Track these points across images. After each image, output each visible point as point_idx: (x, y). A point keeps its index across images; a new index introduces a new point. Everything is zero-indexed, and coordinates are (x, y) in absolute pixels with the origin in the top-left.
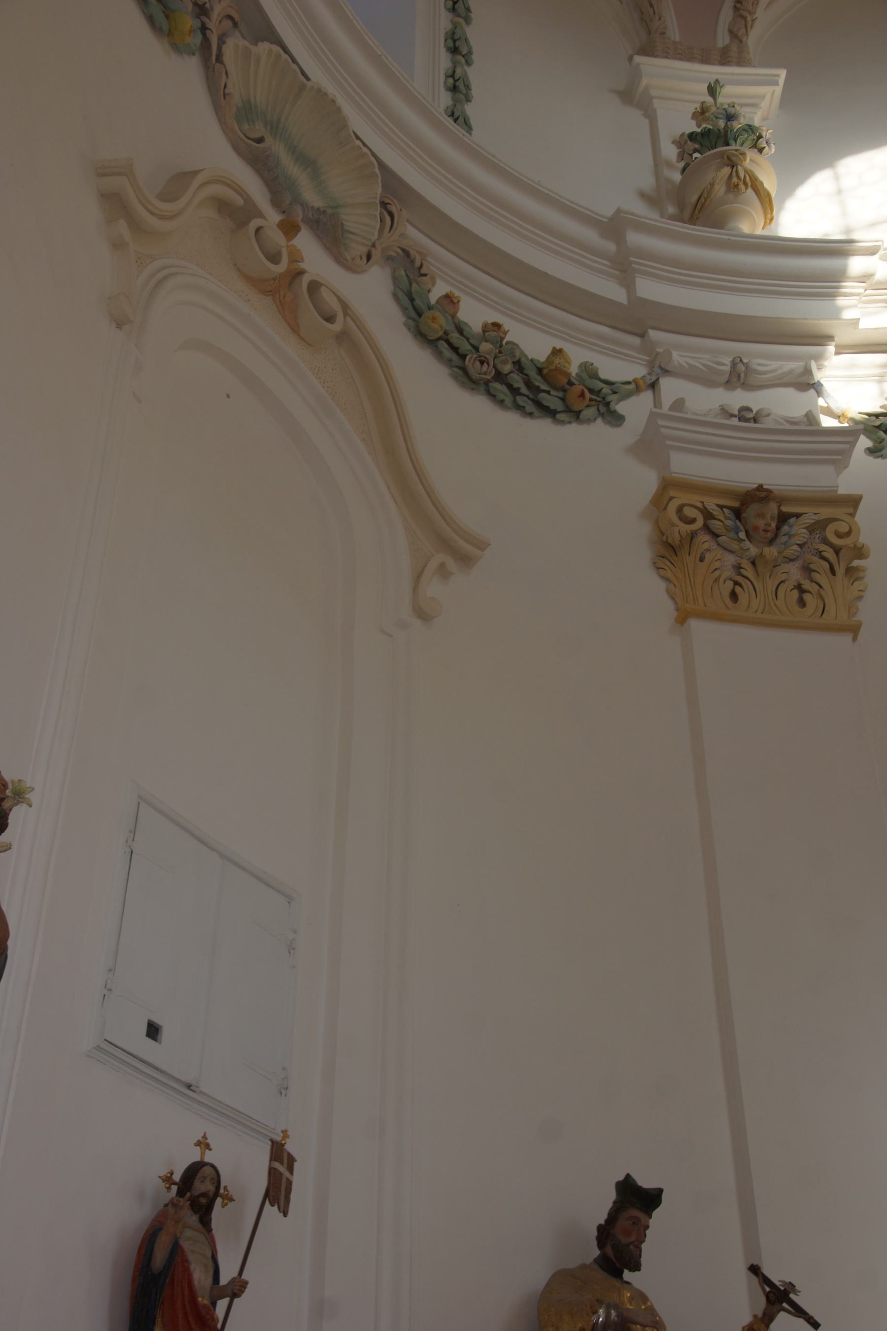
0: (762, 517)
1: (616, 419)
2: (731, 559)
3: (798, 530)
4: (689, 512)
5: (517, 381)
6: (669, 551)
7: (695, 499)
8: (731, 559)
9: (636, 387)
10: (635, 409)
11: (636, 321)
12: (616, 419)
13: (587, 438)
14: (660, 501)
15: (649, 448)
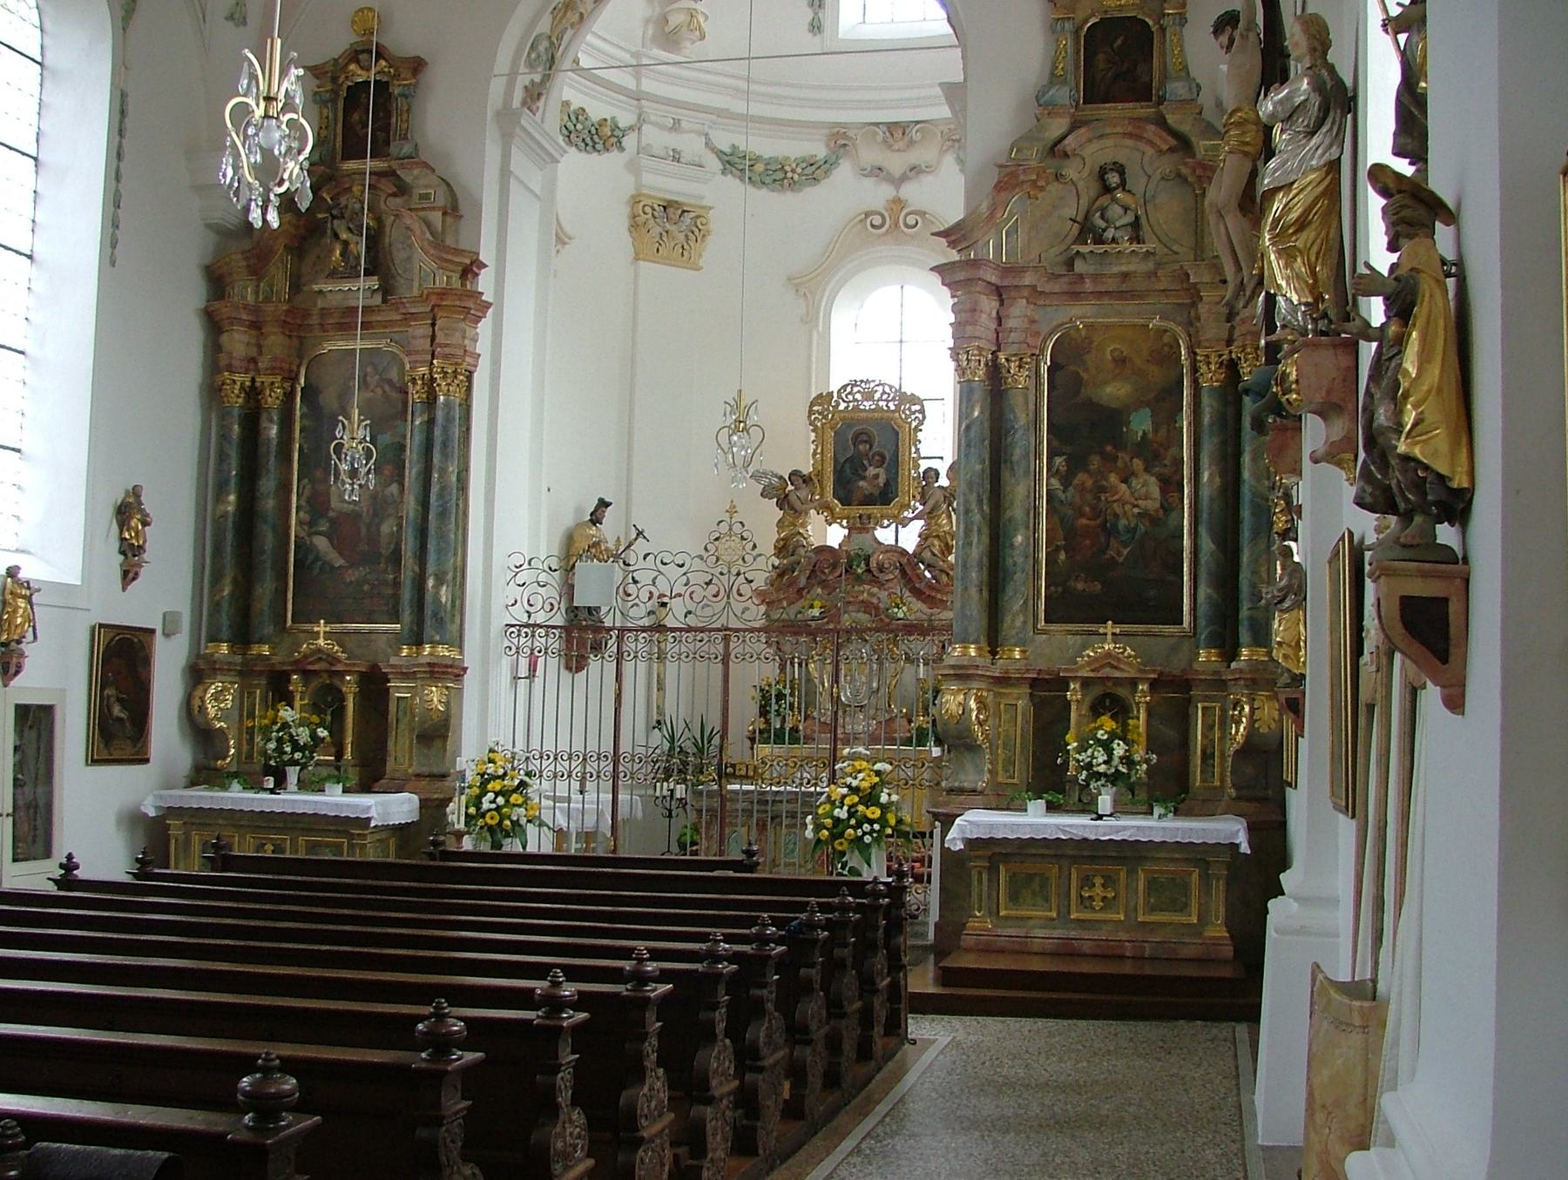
0: (674, 213)
1: (622, 149)
2: (659, 229)
3: (687, 218)
4: (648, 209)
5: (588, 140)
6: (635, 225)
7: (649, 202)
8: (659, 229)
9: (631, 128)
10: (630, 141)
11: (638, 97)
12: (622, 149)
13: (610, 162)
14: (635, 200)
15: (633, 167)
